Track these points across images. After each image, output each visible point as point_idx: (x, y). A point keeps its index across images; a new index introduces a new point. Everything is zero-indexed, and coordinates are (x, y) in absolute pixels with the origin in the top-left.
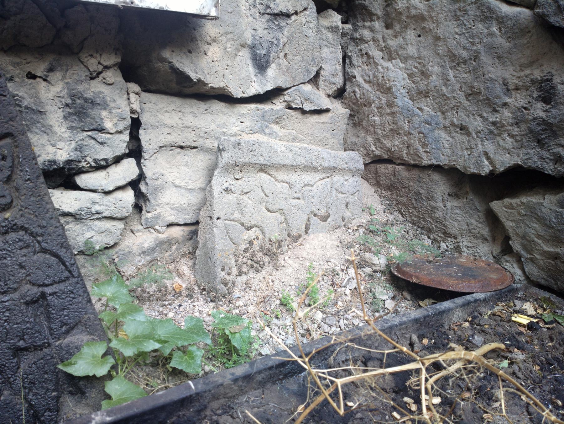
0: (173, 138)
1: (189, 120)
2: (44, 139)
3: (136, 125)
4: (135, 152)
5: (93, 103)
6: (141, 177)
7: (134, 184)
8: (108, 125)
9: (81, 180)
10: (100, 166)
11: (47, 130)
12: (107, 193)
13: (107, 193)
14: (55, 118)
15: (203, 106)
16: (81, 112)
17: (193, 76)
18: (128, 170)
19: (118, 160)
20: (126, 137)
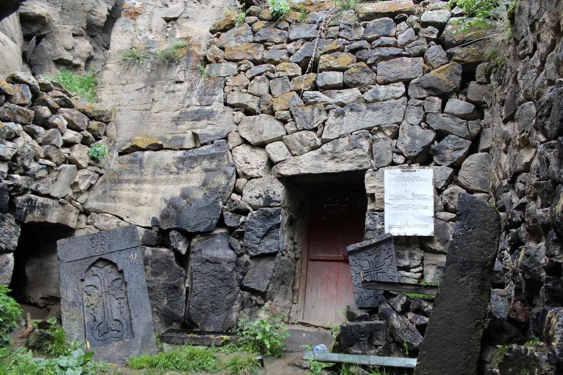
0: (431, 262)
1: (435, 258)
2: (404, 261)
3: (422, 259)
4: (422, 264)
5: (413, 254)
6: (423, 270)
7: (422, 272)
8: (416, 258)
9: (411, 270)
10: (415, 267)
11: (405, 259)
12: (415, 273)
13: (415, 273)
14: (407, 257)
15: (438, 255)
16: (411, 256)
17: (433, 248)
18: (420, 268)
19: (418, 266)
20: (420, 261)
